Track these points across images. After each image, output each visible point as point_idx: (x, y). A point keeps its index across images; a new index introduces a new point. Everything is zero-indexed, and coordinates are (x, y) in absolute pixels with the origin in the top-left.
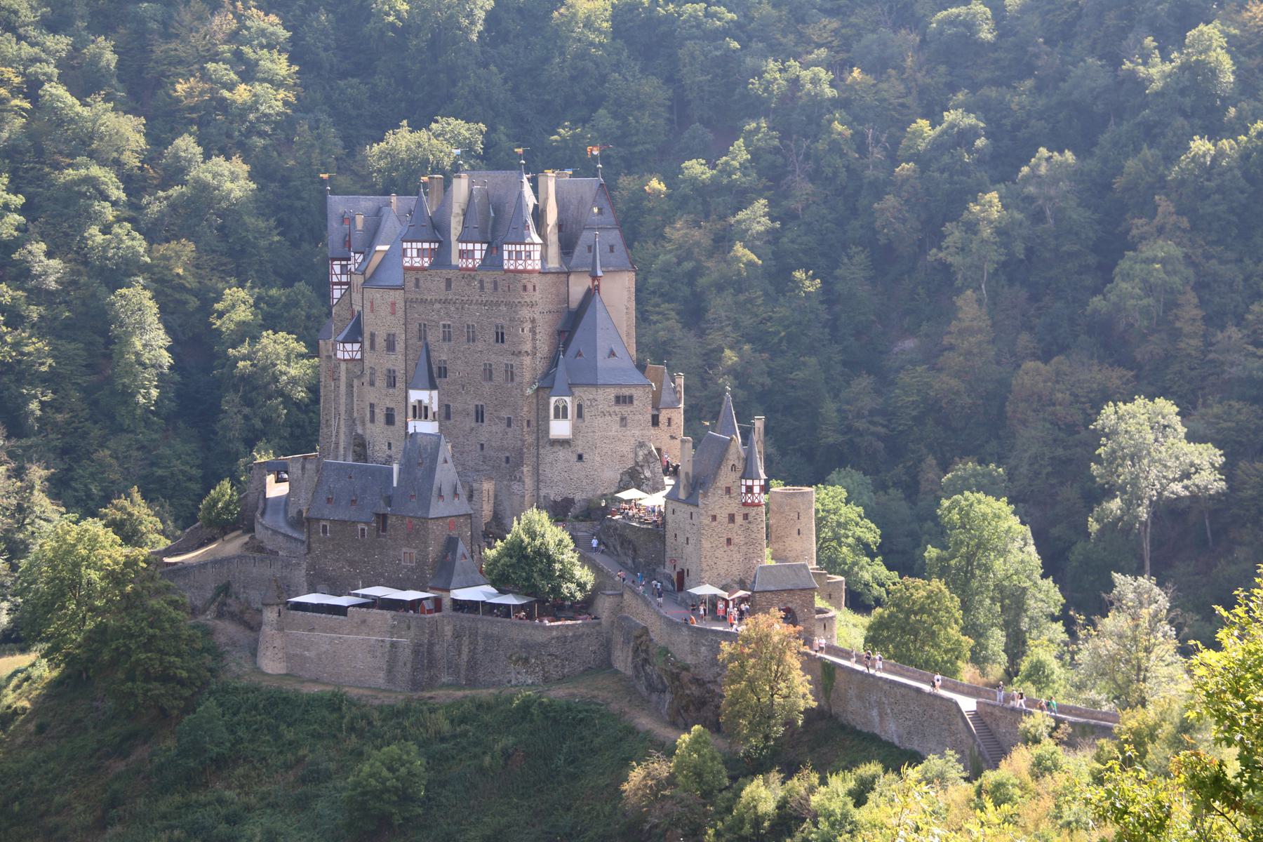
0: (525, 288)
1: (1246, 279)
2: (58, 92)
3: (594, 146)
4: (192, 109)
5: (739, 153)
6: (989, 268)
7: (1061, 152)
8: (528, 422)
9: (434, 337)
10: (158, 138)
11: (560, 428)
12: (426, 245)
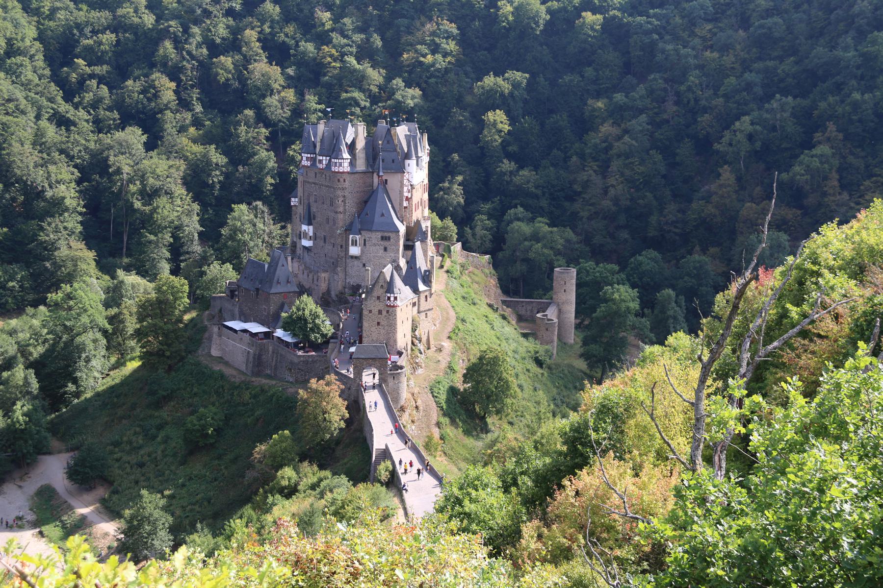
0: (339, 181)
1: (867, 167)
2: (352, 60)
3: (386, 109)
4: (408, 66)
5: (641, 89)
6: (742, 154)
7: (787, 97)
8: (341, 246)
9: (312, 199)
10: (389, 79)
11: (354, 251)
12: (309, 155)
